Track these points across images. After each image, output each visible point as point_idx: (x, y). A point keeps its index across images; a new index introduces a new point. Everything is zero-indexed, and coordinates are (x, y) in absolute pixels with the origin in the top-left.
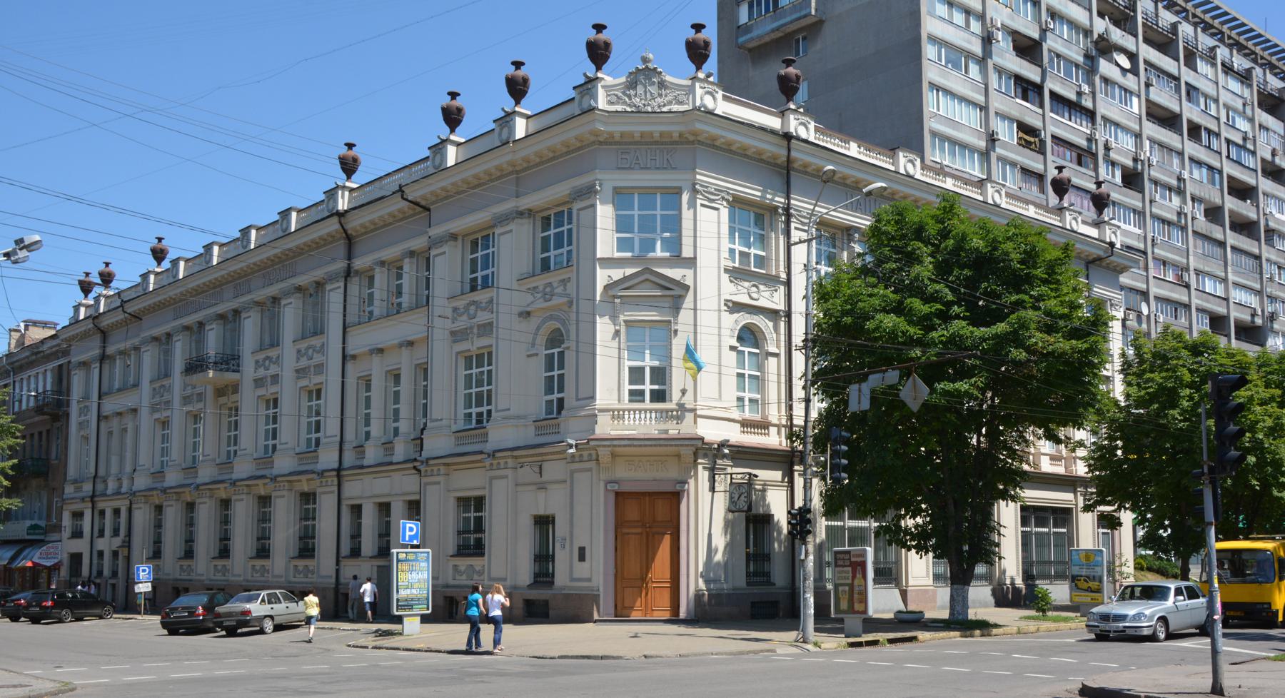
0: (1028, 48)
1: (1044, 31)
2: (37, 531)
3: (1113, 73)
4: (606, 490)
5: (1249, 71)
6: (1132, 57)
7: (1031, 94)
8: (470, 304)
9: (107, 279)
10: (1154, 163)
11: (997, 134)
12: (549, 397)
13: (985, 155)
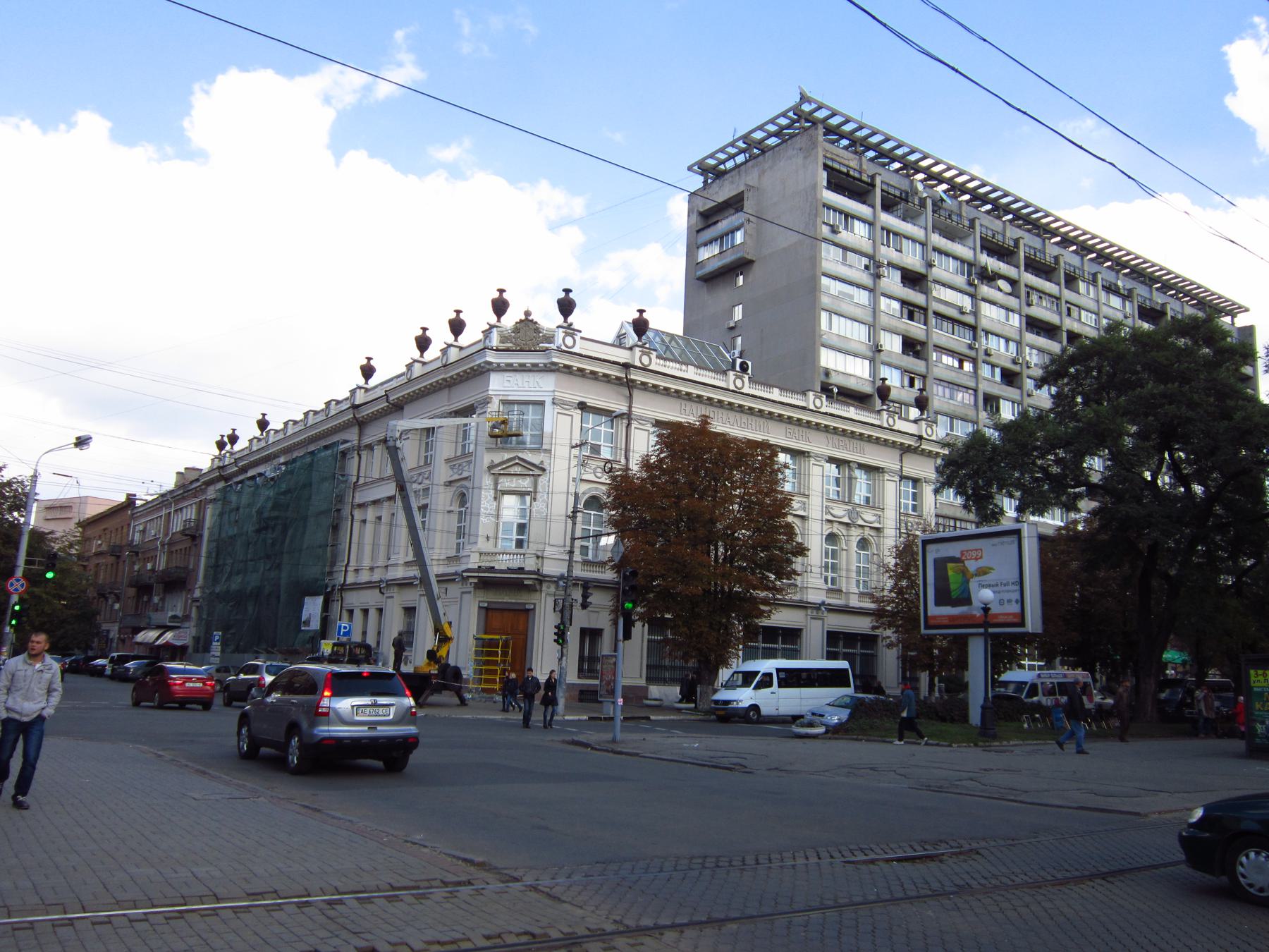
0: (913, 279)
1: (930, 265)
2: (176, 620)
3: (998, 296)
4: (480, 608)
5: (1130, 291)
6: (1013, 282)
7: (916, 315)
8: (420, 474)
9: (233, 439)
10: (1033, 366)
11: (881, 346)
12: (459, 541)
13: (872, 361)
